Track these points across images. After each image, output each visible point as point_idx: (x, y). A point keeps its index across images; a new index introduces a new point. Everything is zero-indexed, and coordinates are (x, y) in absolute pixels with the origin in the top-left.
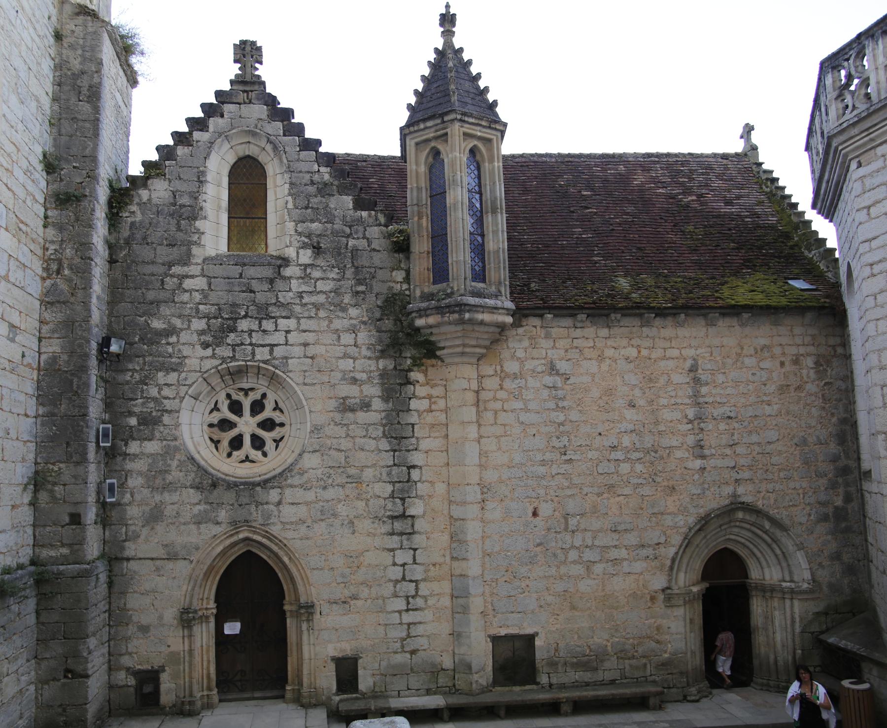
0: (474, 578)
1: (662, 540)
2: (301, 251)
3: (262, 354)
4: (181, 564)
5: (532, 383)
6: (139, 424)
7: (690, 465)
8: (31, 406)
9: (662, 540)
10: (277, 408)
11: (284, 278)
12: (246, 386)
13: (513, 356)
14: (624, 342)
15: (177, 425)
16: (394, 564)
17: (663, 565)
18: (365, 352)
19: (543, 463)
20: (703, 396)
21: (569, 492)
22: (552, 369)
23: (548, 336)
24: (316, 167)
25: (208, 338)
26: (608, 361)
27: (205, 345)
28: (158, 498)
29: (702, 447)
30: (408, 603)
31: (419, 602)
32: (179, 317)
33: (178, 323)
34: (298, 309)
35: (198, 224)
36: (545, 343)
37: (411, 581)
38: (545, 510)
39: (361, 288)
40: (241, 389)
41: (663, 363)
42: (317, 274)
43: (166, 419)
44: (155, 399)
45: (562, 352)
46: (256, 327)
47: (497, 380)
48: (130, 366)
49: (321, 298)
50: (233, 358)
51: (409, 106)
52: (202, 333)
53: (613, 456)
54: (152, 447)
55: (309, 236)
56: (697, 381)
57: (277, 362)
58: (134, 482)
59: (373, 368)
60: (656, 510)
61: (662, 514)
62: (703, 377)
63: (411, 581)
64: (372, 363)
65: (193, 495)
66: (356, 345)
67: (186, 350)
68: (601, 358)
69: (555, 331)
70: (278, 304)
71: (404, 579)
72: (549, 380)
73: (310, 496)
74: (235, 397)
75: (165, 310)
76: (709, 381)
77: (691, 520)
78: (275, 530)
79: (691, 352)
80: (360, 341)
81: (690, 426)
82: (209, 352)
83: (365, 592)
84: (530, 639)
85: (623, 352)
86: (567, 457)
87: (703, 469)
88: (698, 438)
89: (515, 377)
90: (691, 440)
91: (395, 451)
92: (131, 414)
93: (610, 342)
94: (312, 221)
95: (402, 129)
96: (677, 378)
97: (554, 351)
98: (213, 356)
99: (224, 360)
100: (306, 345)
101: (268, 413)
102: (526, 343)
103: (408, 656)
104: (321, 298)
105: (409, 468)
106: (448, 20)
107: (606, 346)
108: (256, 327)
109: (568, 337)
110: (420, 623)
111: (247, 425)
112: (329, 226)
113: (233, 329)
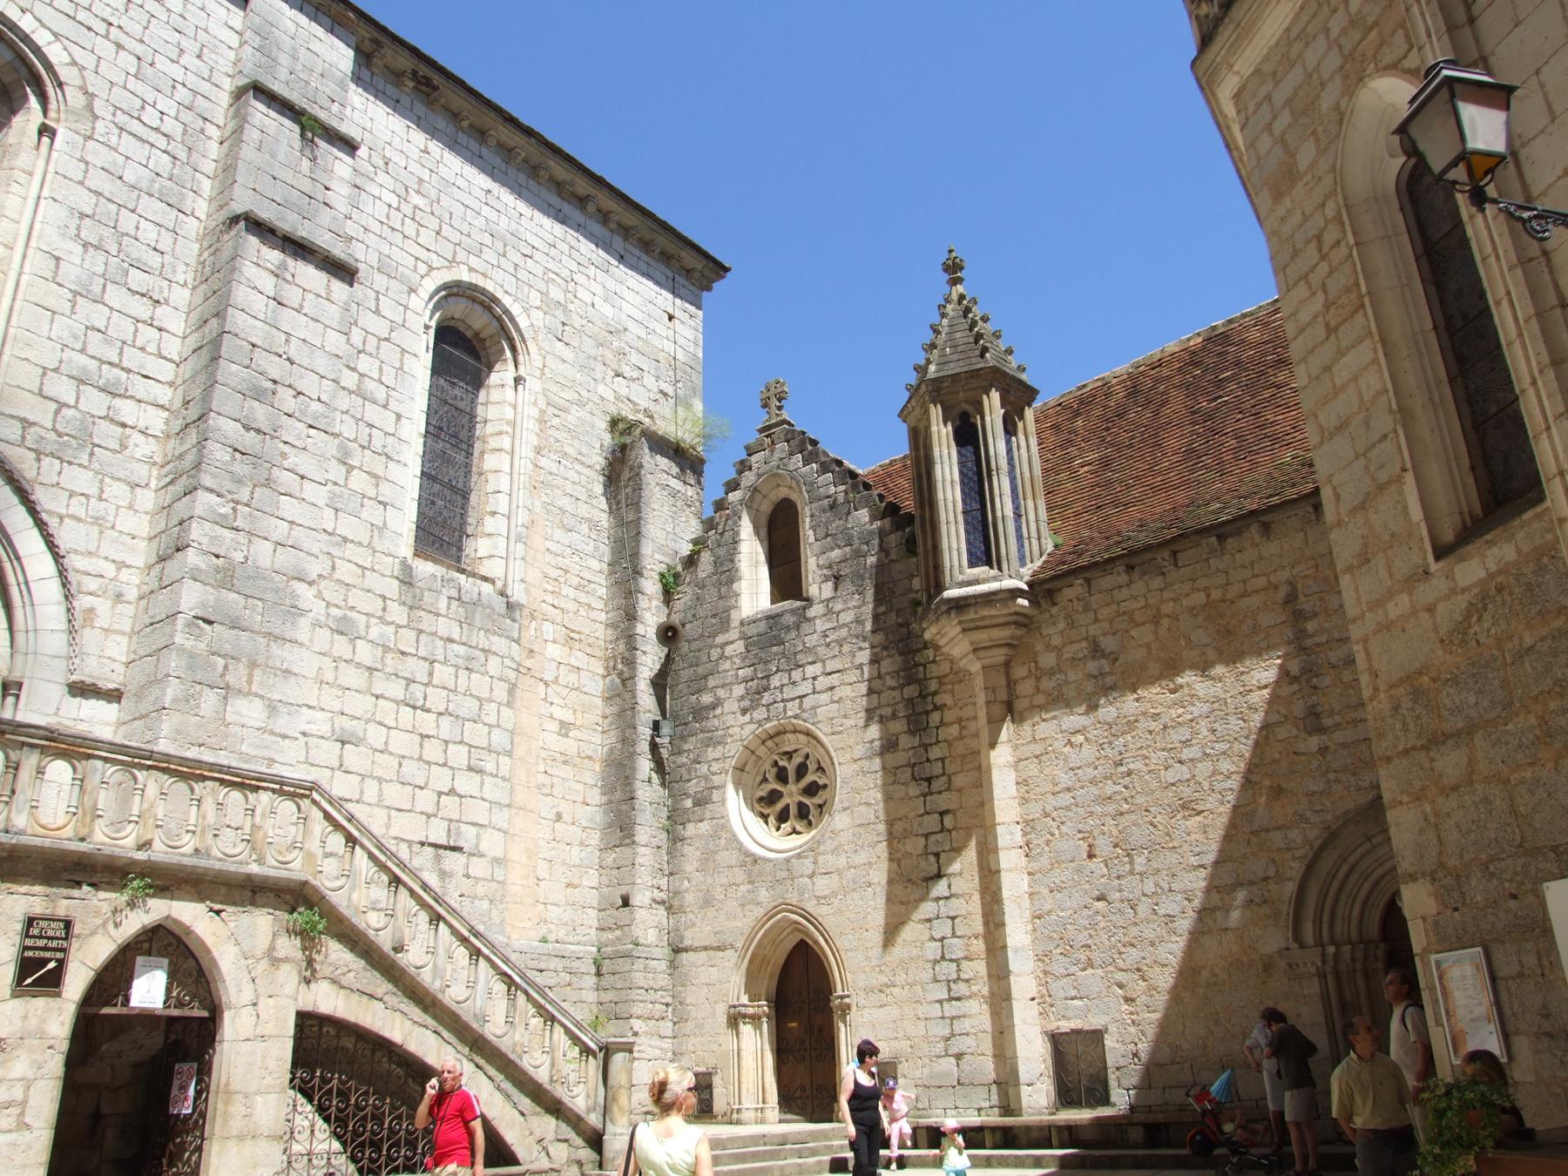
0: (1016, 951)
1: (1271, 872)
2: (824, 586)
3: (792, 709)
4: (729, 953)
5: (1072, 676)
6: (695, 805)
7: (1302, 747)
8: (596, 797)
9: (1271, 872)
10: (820, 769)
11: (809, 620)
12: (788, 749)
13: (1049, 647)
14: (1187, 587)
15: (723, 802)
16: (933, 939)
17: (1276, 914)
18: (890, 682)
19: (1093, 782)
20: (1310, 636)
21: (1133, 817)
22: (1096, 651)
23: (1087, 609)
24: (832, 490)
25: (746, 703)
26: (1165, 622)
27: (744, 711)
28: (709, 880)
29: (1317, 715)
30: (950, 990)
31: (961, 989)
32: (723, 686)
33: (721, 693)
34: (821, 650)
35: (735, 586)
36: (1083, 619)
37: (951, 960)
38: (1103, 846)
39: (883, 609)
40: (786, 753)
41: (1244, 602)
42: (838, 607)
43: (715, 796)
44: (706, 778)
45: (1106, 625)
46: (786, 681)
47: (1032, 681)
48: (686, 747)
49: (844, 632)
50: (768, 719)
51: (909, 388)
52: (742, 698)
53: (1187, 754)
54: (704, 827)
55: (830, 567)
56: (1298, 616)
57: (805, 715)
58: (690, 867)
59: (898, 699)
60: (1256, 827)
61: (1267, 830)
62: (1307, 607)
63: (951, 960)
64: (896, 693)
65: (739, 875)
66: (879, 677)
67: (730, 720)
68: (1156, 621)
69: (1095, 600)
70: (808, 650)
71: (943, 957)
72: (1092, 666)
73: (842, 861)
74: (781, 763)
75: (711, 683)
76: (1317, 610)
77: (1313, 834)
78: (810, 906)
79: (1284, 575)
80: (883, 671)
81: (1295, 687)
82: (748, 717)
83: (901, 978)
84: (1097, 1036)
85: (1185, 602)
86: (1124, 769)
87: (1323, 750)
88: (1310, 703)
89: (1052, 673)
90: (1298, 708)
91: (924, 795)
92: (687, 795)
93: (1166, 595)
94: (832, 549)
95: (903, 414)
96: (1266, 619)
97: (1096, 626)
98: (751, 722)
99: (760, 723)
100: (832, 688)
101: (810, 777)
102: (1062, 625)
103: (953, 1060)
104: (844, 632)
105: (942, 814)
106: (953, 269)
107: (1162, 601)
108: (786, 681)
109: (1113, 601)
110: (964, 1016)
111: (792, 794)
112: (847, 549)
113: (766, 689)
